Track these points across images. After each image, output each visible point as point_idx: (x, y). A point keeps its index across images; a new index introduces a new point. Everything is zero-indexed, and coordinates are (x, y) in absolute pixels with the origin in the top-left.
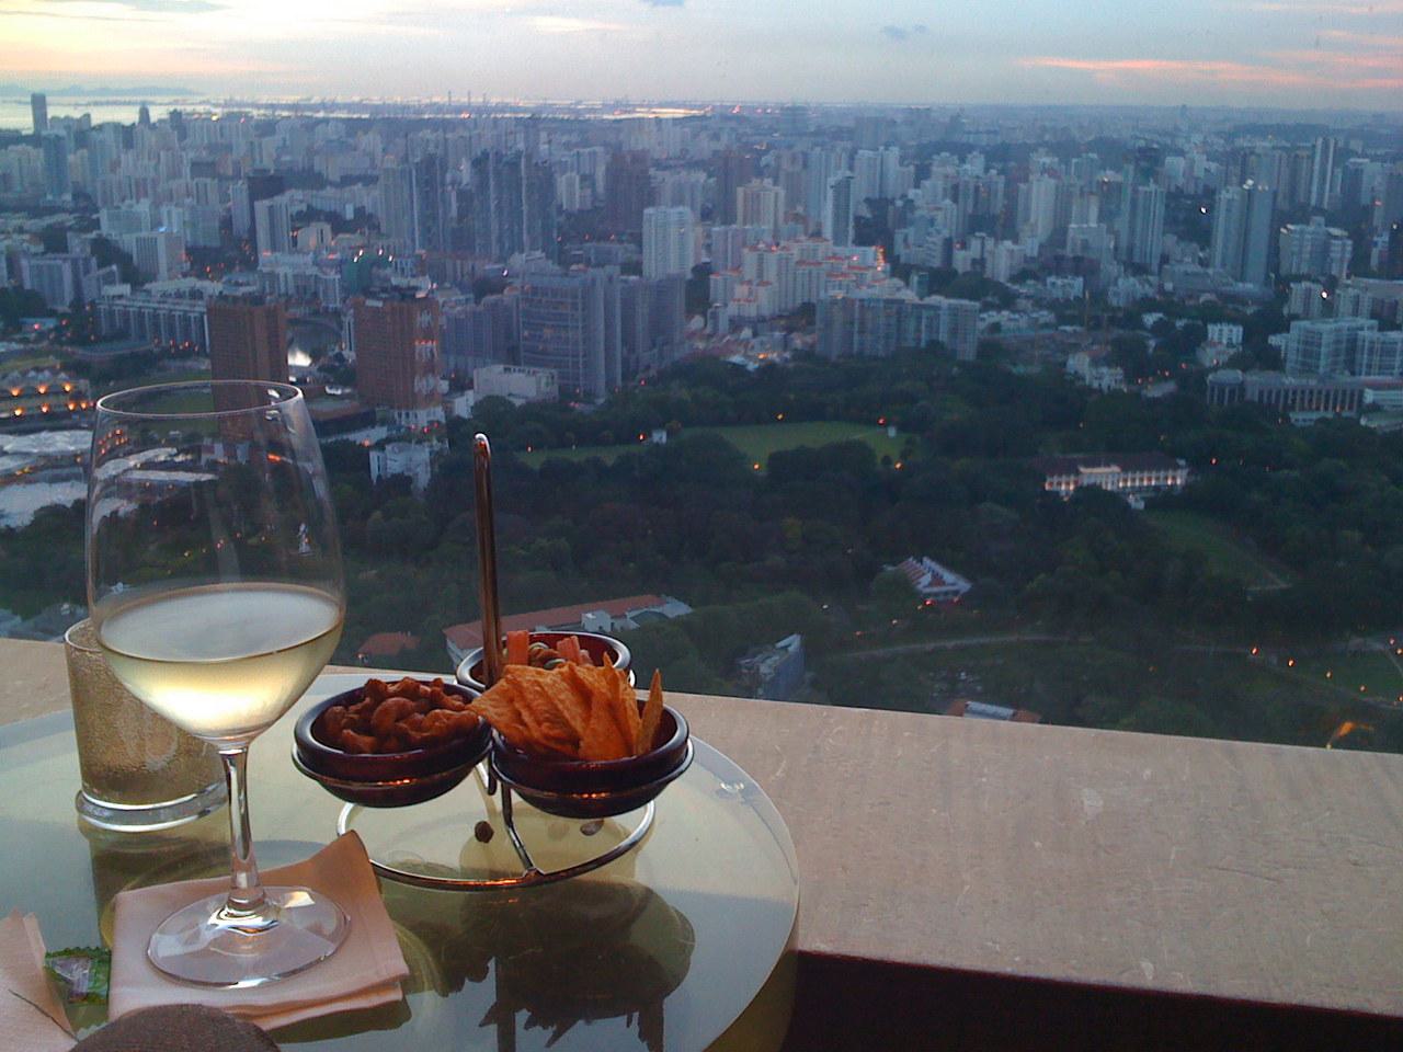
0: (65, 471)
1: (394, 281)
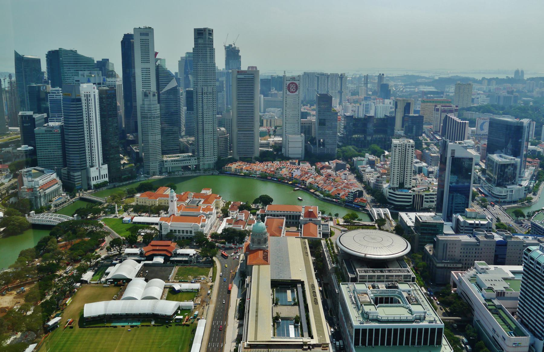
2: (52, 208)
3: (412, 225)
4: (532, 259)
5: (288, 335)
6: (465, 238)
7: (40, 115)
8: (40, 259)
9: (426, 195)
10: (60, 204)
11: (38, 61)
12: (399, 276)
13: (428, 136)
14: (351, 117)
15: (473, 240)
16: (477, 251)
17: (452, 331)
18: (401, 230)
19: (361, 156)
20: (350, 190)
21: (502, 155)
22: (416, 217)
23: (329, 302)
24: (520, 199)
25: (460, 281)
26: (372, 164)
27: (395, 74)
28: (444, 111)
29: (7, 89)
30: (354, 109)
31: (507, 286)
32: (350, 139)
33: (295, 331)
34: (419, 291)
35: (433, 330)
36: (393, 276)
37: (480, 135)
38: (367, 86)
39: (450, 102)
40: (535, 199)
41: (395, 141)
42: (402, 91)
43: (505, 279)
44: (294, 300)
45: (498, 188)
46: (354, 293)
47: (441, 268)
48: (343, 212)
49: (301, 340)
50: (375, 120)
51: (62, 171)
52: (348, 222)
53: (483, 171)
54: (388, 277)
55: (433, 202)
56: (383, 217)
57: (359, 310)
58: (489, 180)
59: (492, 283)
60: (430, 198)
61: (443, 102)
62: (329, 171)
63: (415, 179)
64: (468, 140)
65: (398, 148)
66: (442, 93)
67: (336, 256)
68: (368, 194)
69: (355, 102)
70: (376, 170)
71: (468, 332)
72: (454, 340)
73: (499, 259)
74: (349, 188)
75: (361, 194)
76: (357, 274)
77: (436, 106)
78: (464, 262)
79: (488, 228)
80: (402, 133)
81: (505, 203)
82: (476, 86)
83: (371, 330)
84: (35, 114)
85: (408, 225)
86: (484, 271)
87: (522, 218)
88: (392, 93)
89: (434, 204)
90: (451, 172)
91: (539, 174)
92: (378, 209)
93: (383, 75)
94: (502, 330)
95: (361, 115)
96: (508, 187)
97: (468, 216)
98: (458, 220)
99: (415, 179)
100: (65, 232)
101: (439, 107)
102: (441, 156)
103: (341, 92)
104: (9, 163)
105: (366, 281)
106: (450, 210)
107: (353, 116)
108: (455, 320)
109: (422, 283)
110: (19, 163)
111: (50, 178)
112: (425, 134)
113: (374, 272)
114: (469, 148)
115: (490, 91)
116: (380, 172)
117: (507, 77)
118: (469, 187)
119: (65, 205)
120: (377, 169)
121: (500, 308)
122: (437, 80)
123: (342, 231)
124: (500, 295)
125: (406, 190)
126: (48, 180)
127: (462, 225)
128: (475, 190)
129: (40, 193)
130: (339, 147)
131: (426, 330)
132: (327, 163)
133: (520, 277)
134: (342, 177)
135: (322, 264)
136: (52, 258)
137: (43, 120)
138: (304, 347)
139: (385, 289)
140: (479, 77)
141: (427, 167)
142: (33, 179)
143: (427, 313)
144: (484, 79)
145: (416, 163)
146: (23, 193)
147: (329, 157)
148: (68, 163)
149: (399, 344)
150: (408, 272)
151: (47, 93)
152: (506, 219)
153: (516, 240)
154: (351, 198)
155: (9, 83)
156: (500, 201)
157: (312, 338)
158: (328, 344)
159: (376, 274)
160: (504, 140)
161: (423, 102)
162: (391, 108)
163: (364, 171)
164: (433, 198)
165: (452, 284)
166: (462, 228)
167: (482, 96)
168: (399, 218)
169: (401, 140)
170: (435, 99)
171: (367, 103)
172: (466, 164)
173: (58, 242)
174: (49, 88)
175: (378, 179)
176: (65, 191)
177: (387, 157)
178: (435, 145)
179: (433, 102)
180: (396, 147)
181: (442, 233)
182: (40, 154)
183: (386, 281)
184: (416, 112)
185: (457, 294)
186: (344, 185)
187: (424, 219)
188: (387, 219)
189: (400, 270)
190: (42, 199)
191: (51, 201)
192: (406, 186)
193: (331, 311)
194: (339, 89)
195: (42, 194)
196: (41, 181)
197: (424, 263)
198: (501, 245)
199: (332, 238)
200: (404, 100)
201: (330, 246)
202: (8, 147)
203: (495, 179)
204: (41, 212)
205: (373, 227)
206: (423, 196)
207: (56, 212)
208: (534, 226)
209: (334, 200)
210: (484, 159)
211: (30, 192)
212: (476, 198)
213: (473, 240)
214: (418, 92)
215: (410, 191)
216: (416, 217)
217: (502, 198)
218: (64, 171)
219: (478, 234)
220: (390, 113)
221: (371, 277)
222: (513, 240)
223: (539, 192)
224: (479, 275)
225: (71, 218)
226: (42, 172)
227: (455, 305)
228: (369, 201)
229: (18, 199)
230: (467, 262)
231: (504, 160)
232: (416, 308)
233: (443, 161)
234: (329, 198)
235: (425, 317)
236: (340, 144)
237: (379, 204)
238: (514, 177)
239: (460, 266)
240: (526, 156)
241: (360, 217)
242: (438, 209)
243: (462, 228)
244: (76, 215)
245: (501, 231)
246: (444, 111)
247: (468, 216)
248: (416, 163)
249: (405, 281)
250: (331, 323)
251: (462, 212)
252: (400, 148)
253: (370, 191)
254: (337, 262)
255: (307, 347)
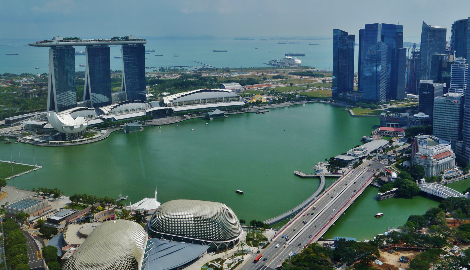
2: (442, 180)
7: (440, 84)
8: (427, 229)
10: (451, 178)
11: (444, 31)
29: (409, 58)
51: (457, 144)
84: (435, 84)
100: (455, 208)
104: (405, 128)
110: (415, 129)
111: (445, 149)
119: (456, 180)
126: (443, 150)
129: (433, 162)
136: (438, 231)
137: (442, 90)
142: (428, 147)
146: (417, 159)
148: (464, 136)
151: (449, 64)
155: (412, 52)
173: (447, 216)
174: (452, 58)
176: (458, 166)
182: (436, 122)
190: (434, 169)
191: (442, 173)
195: (435, 164)
196: (435, 150)
202: (405, 112)
204: (431, 181)
207: (446, 184)
211: (423, 159)
218: (459, 144)
225: (462, 195)
226: (437, 141)
229: (411, 164)
244: (467, 193)
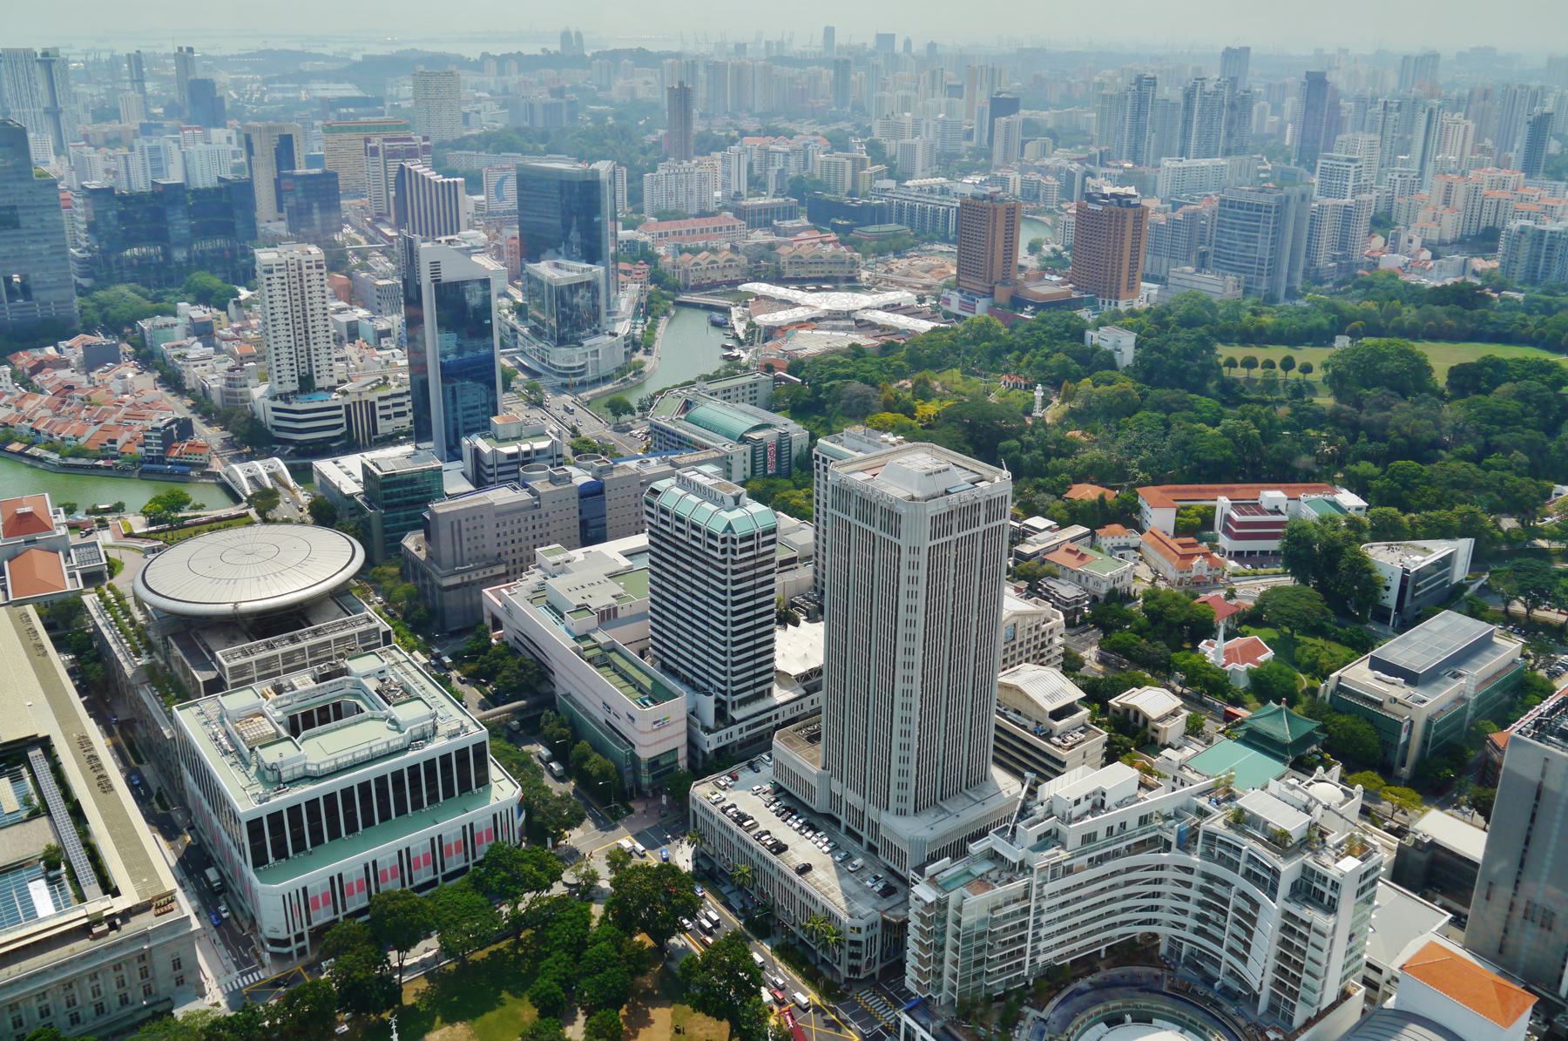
0: (842, 323)
1: (1108, 190)
3: (358, 489)
4: (664, 511)
5: (31, 913)
6: (501, 496)
9: (381, 399)
12: (346, 639)
13: (361, 232)
14: (108, 192)
15: (522, 496)
16: (537, 522)
17: (510, 740)
18: (329, 512)
19: (163, 313)
20: (149, 424)
21: (561, 261)
22: (364, 466)
23: (147, 771)
24: (618, 369)
25: (509, 609)
26: (203, 332)
27: (229, 47)
28: (394, 154)
30: (112, 164)
31: (621, 591)
32: (118, 262)
33: (53, 892)
34: (405, 664)
35: (462, 754)
36: (328, 643)
37: (498, 213)
38: (142, 90)
39: (407, 127)
40: (650, 363)
41: (264, 256)
42: (260, 102)
43: (613, 576)
44: (26, 801)
45: (563, 349)
46: (223, 723)
47: (456, 587)
48: (138, 496)
49: (82, 913)
50: (188, 196)
52: (161, 521)
53: (520, 310)
54: (313, 650)
55: (403, 414)
56: (268, 483)
57: (248, 765)
58: (537, 332)
59: (585, 593)
60: (395, 405)
61: (385, 128)
62: (64, 375)
63: (343, 359)
64: (471, 232)
65: (276, 274)
66: (381, 101)
67: (141, 632)
68: (208, 424)
69: (113, 142)
70: (218, 350)
71: (547, 729)
72: (517, 761)
73: (591, 532)
74: (142, 417)
75: (185, 428)
76: (221, 665)
77: (367, 140)
78: (510, 558)
79: (554, 457)
80: (281, 228)
81: (583, 384)
82: (468, 78)
83: (294, 811)
85: (346, 492)
86: (561, 569)
87: (629, 417)
88: (227, 107)
89: (405, 422)
90: (440, 324)
91: (650, 301)
92: (248, 465)
93: (190, 50)
94: (624, 699)
95: (141, 184)
96: (586, 343)
97: (501, 436)
98: (477, 452)
99: (343, 359)
101: (376, 142)
102: (405, 282)
103: (54, 113)
105: (252, 680)
106: (451, 429)
107: (110, 190)
108: (514, 711)
109: (410, 640)
112: (353, 226)
113: (270, 647)
114: (474, 253)
115: (506, 88)
116: (233, 354)
117: (544, 50)
118: (490, 360)
120: (224, 345)
121: (613, 649)
122: (356, 65)
123: (146, 552)
124: (608, 617)
125: (322, 395)
127: (489, 462)
128: (508, 364)
130: (83, 292)
131: (446, 759)
132: (51, 350)
133: (644, 562)
134: (112, 387)
135: (99, 667)
138: (96, 930)
139: (313, 685)
140: (472, 52)
141: (370, 320)
143: (440, 714)
144: (485, 56)
145: (339, 311)
147: (55, 331)
149: (381, 820)
150: (370, 620)
152: (594, 428)
153: (622, 474)
154: (156, 448)
156: (571, 381)
157: (116, 893)
158: (172, 893)
159: (279, 651)
160: (557, 222)
161: (329, 130)
162: (235, 155)
163: (182, 357)
164: (402, 404)
165: (488, 622)
166: (490, 471)
167: (488, 104)
168: (316, 479)
169: (280, 249)
170: (362, 119)
171: (154, 143)
172: (474, 300)
175: (232, 375)
177: (247, 305)
178: (384, 253)
179: (359, 129)
180: (271, 272)
181: (442, 495)
183: (312, 664)
184: (313, 161)
185: (506, 643)
186: (124, 410)
187: (388, 468)
188: (281, 489)
189: (345, 623)
192: (318, 384)
193: (160, 798)
194: (46, 103)
197: (409, 586)
198: (592, 493)
199: (117, 581)
200: (270, 129)
201: (116, 606)
203: (552, 328)
205: (241, 520)
206: (373, 404)
208: (657, 431)
209: (101, 462)
210: (518, 278)
212: (513, 384)
213: (522, 496)
214: (308, 103)
215: (334, 396)
216: (364, 466)
217: (575, 375)
219: (533, 478)
220: (237, 169)
221: (265, 664)
222: (616, 474)
223: (657, 345)
224: (550, 581)
227: (505, 673)
228: (216, 447)
230: (517, 556)
231: (567, 274)
232: (408, 713)
233: (412, 299)
234: (81, 461)
235: (435, 728)
236: (86, 282)
237: (248, 449)
238: (596, 316)
239: (502, 569)
240: (616, 259)
241: (196, 500)
242: (420, 432)
243: (490, 471)
245: (586, 458)
246: (394, 154)
247: (501, 436)
248: (339, 311)
249: (365, 649)
250: (165, 827)
251: (484, 428)
252: (284, 274)
253: (210, 414)
254: (150, 647)
255: (105, 926)
